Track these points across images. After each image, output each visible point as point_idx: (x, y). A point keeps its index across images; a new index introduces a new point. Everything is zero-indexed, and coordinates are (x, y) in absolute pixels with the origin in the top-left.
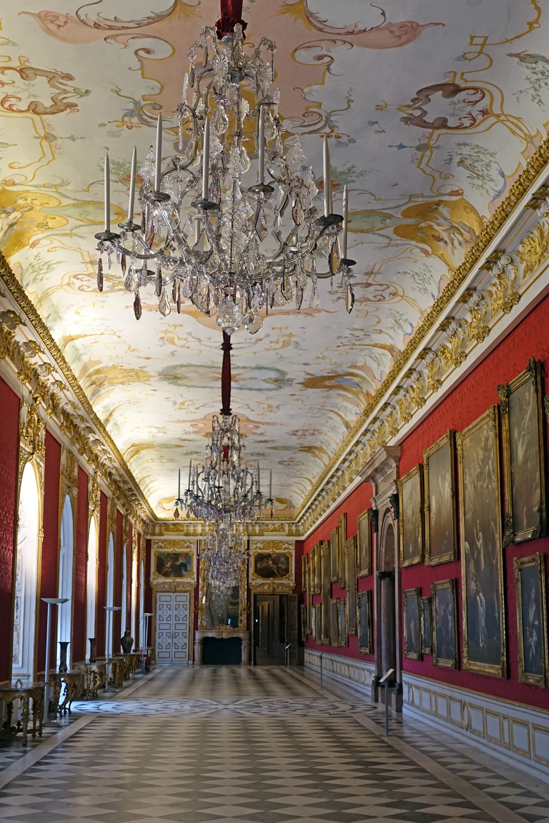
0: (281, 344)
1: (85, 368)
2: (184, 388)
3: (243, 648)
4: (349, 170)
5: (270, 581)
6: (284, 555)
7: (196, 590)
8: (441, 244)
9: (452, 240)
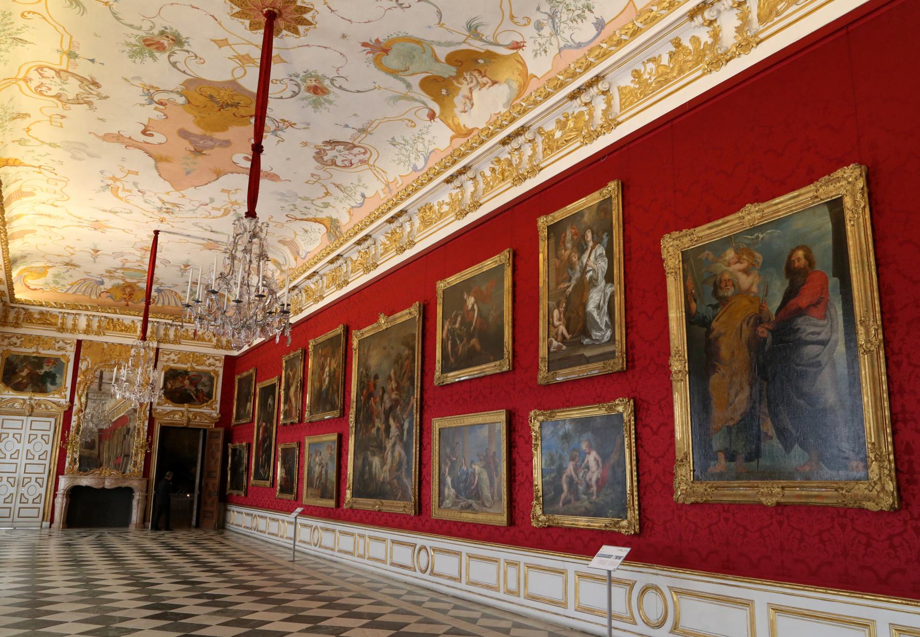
3: (135, 503)
5: (184, 408)
6: (207, 373)
7: (68, 415)
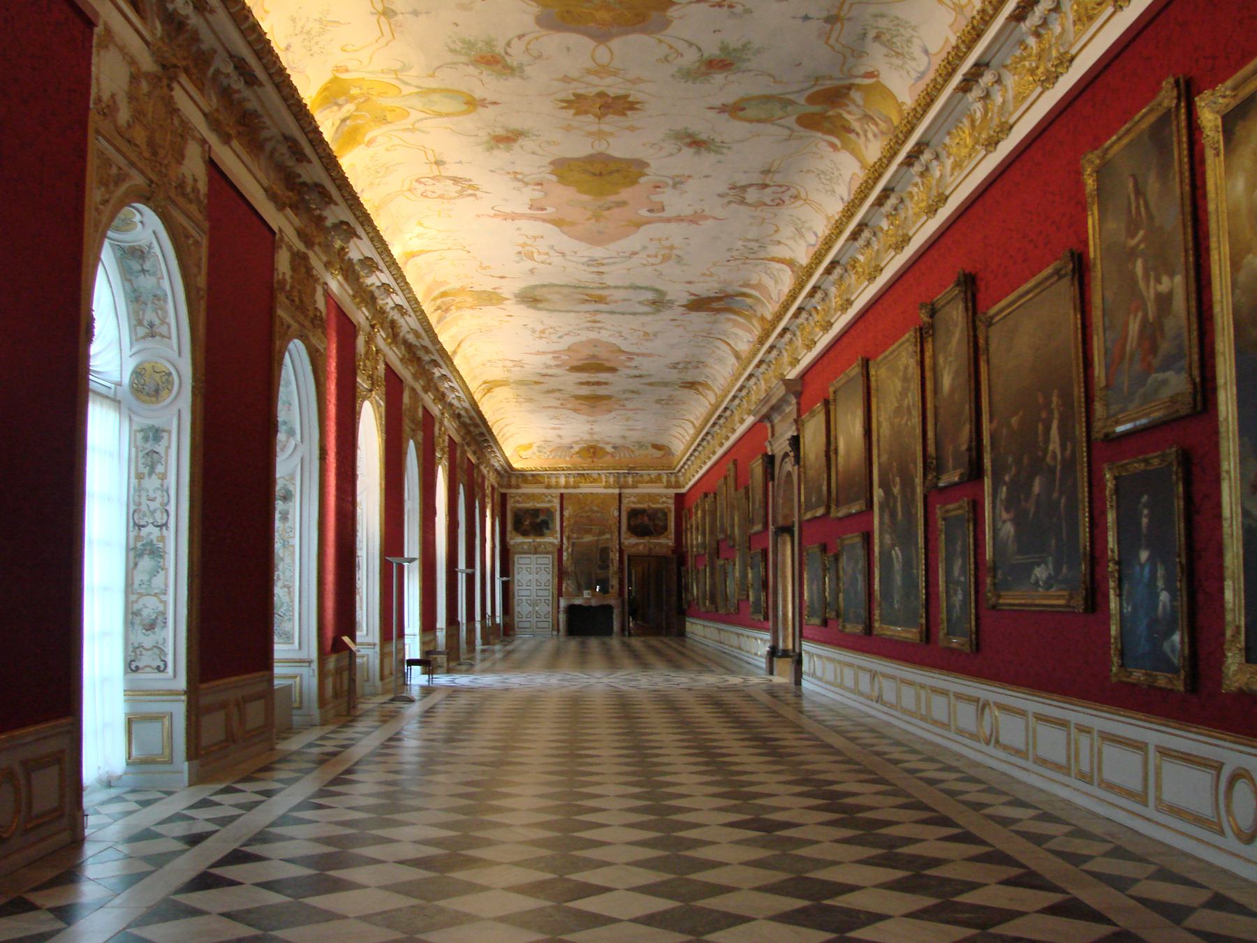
0: (660, 258)
1: (429, 291)
2: (544, 313)
4: (744, 46)
6: (661, 510)
7: (560, 551)
8: (853, 136)
9: (865, 132)
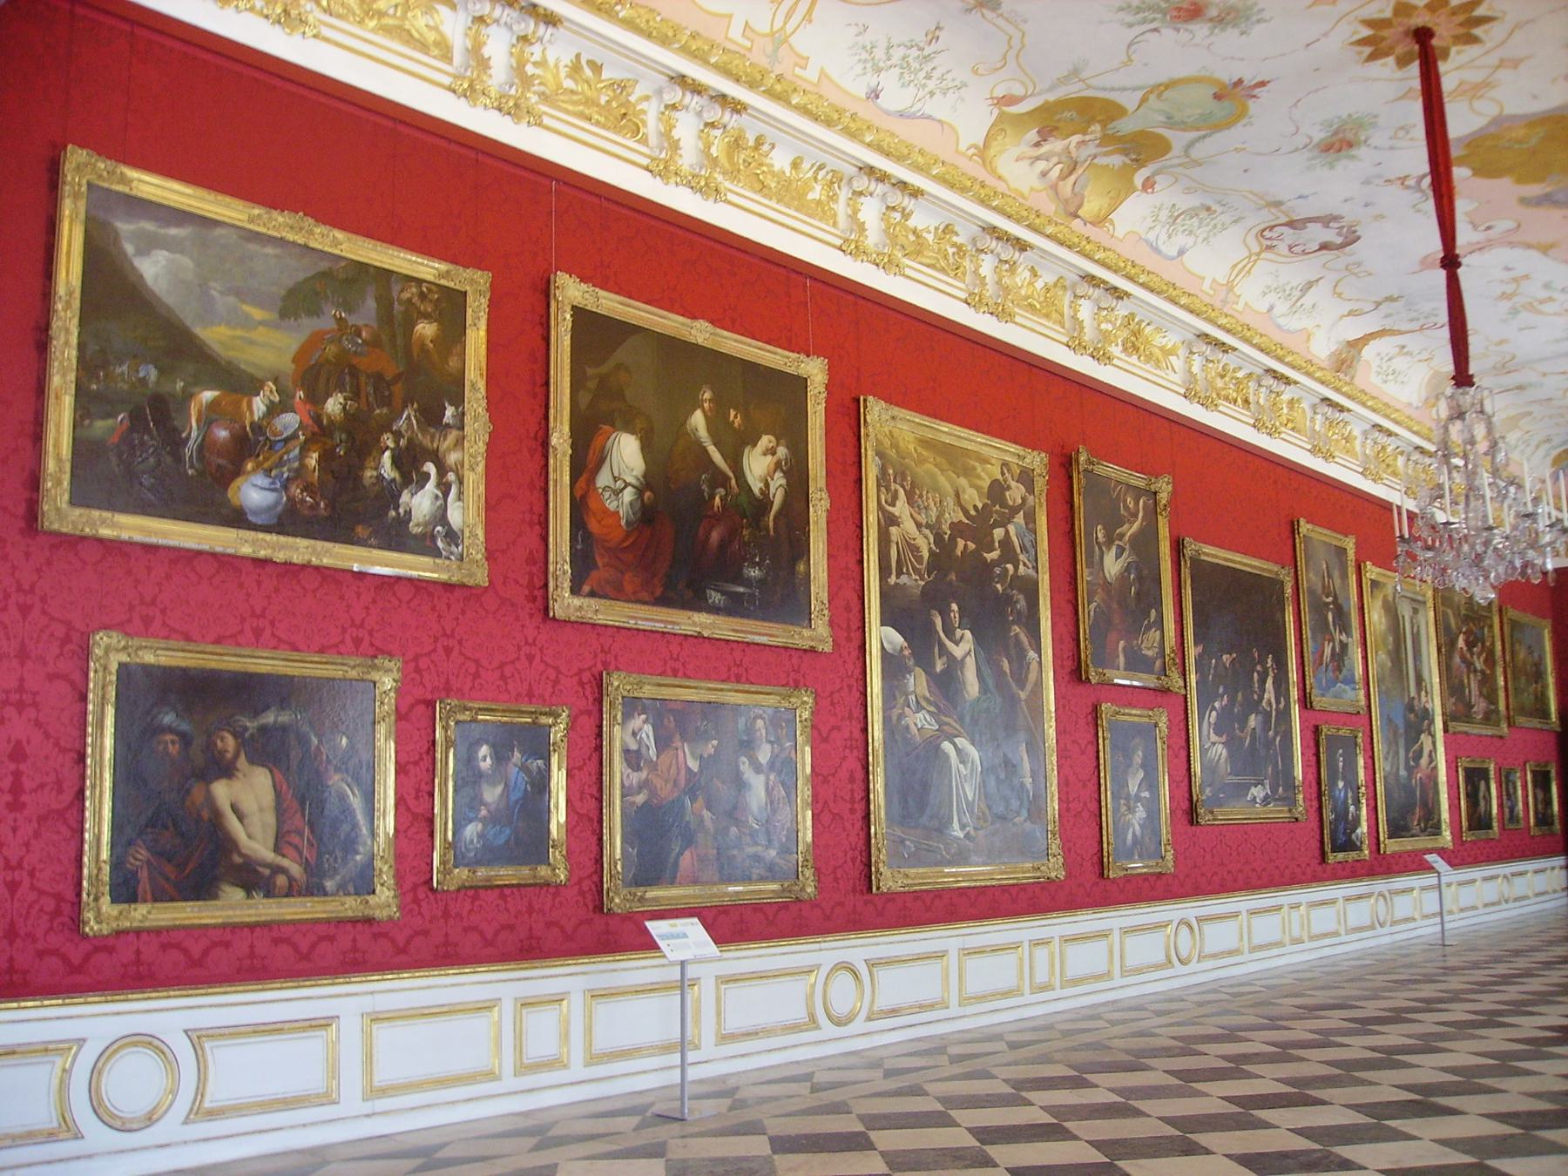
8: (1033, 135)
